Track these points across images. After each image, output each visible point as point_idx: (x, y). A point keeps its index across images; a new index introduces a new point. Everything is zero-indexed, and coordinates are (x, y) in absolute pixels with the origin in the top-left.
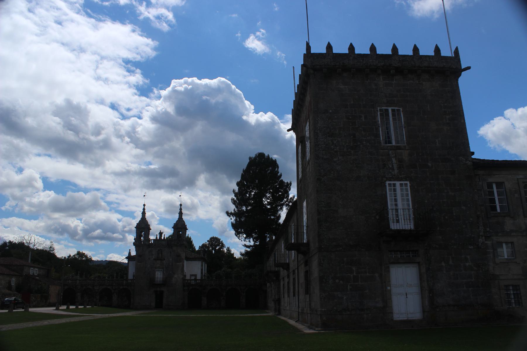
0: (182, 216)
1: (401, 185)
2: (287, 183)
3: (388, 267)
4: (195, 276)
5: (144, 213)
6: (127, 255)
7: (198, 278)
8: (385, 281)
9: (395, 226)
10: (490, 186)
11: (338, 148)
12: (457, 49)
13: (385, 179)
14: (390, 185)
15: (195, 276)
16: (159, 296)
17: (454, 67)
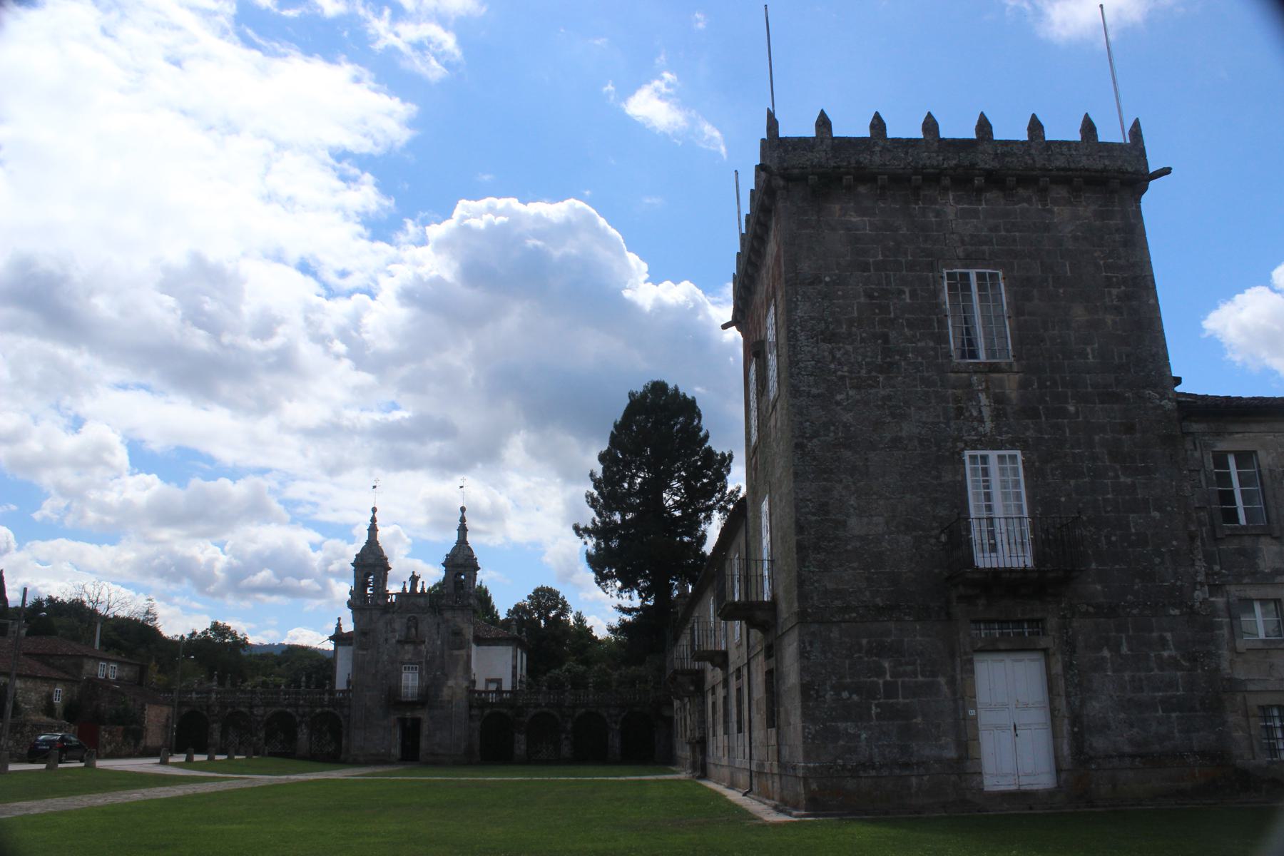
1: (1001, 458)
2: (723, 454)
3: (971, 662)
4: (499, 681)
5: (373, 529)
6: (333, 632)
8: (962, 695)
9: (987, 560)
10: (1221, 460)
11: (846, 369)
12: (1136, 124)
13: (961, 445)
14: (973, 458)
15: (499, 681)
16: (411, 732)
17: (1130, 169)
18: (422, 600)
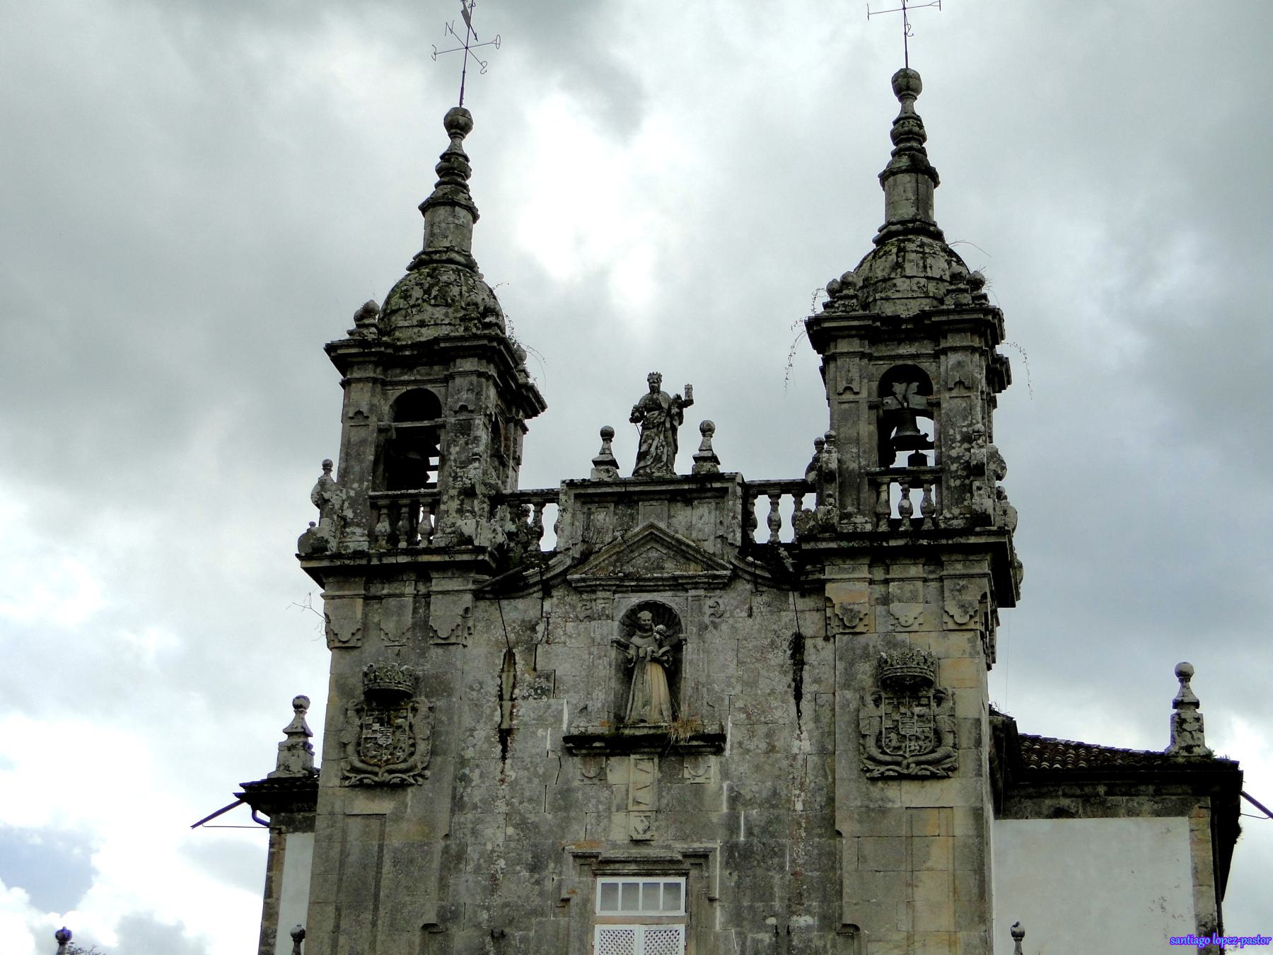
0: (924, 202)
6: (263, 767)
18: (698, 523)
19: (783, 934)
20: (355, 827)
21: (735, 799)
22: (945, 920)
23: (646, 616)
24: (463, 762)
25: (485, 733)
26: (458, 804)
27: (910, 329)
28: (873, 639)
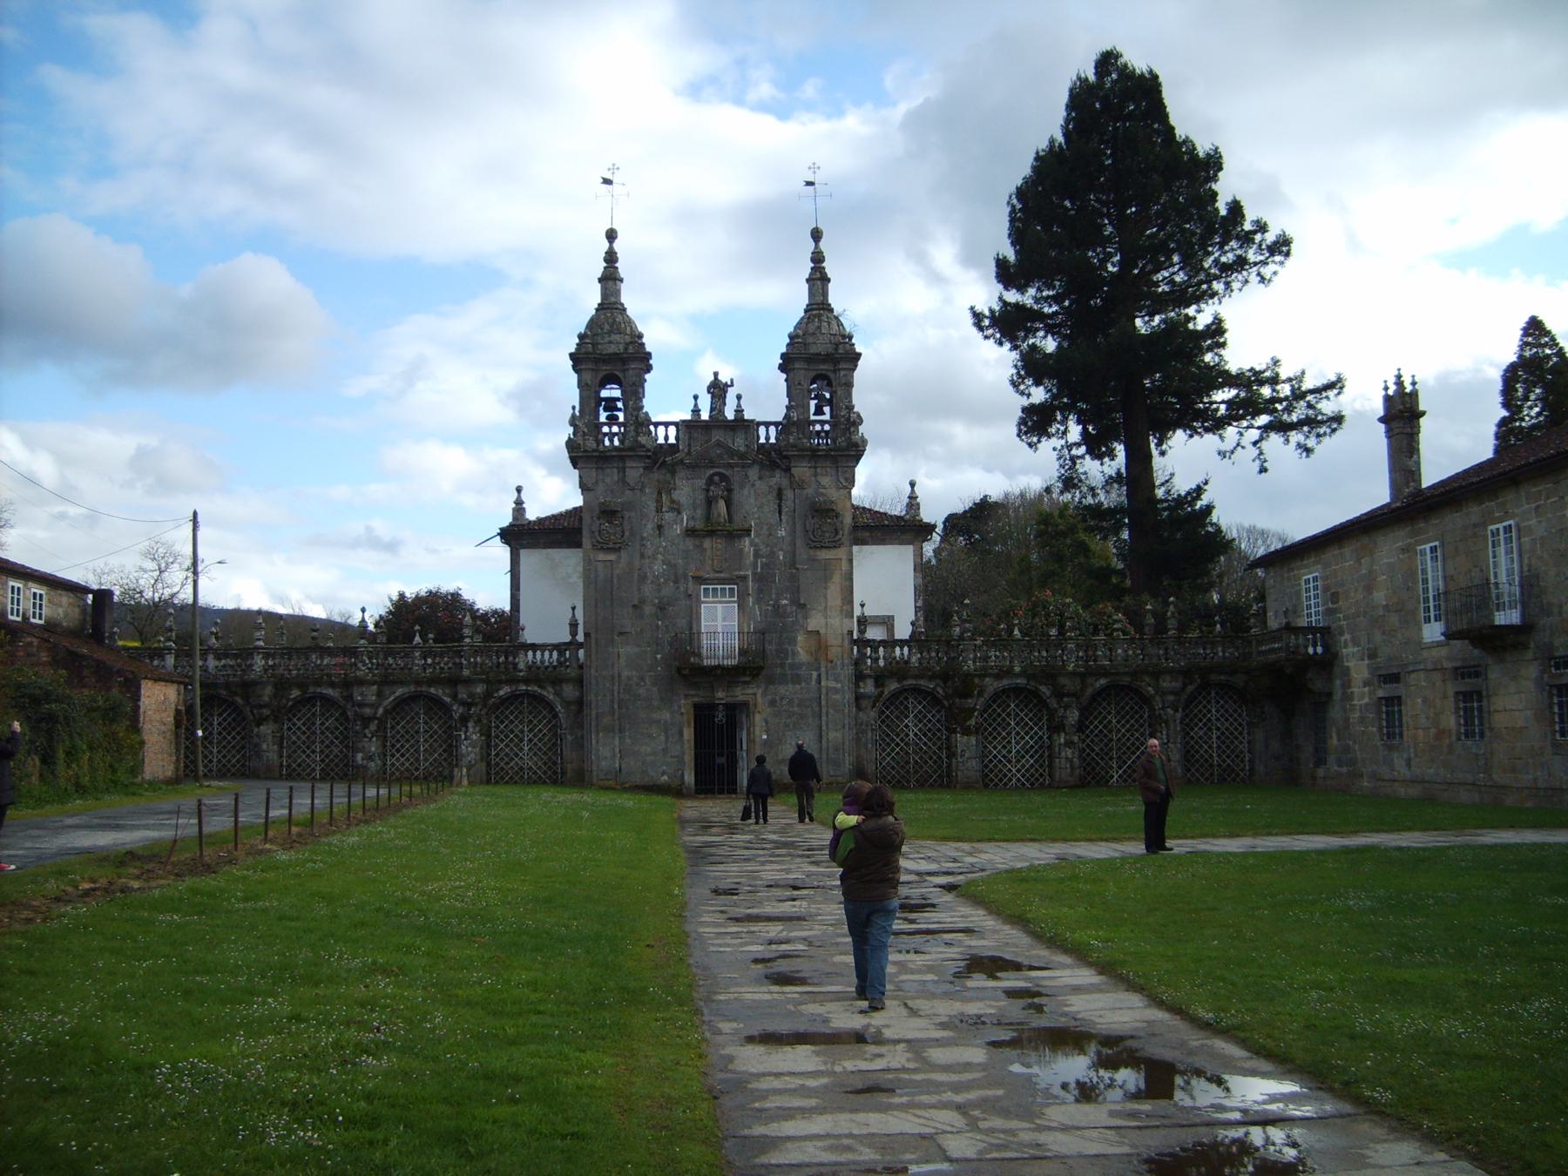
0: (825, 294)
4: (887, 622)
6: (506, 520)
7: (898, 636)
15: (887, 622)
19: (776, 607)
20: (600, 566)
21: (757, 555)
22: (839, 602)
23: (716, 478)
24: (643, 539)
25: (649, 528)
26: (642, 556)
27: (820, 355)
28: (810, 491)
